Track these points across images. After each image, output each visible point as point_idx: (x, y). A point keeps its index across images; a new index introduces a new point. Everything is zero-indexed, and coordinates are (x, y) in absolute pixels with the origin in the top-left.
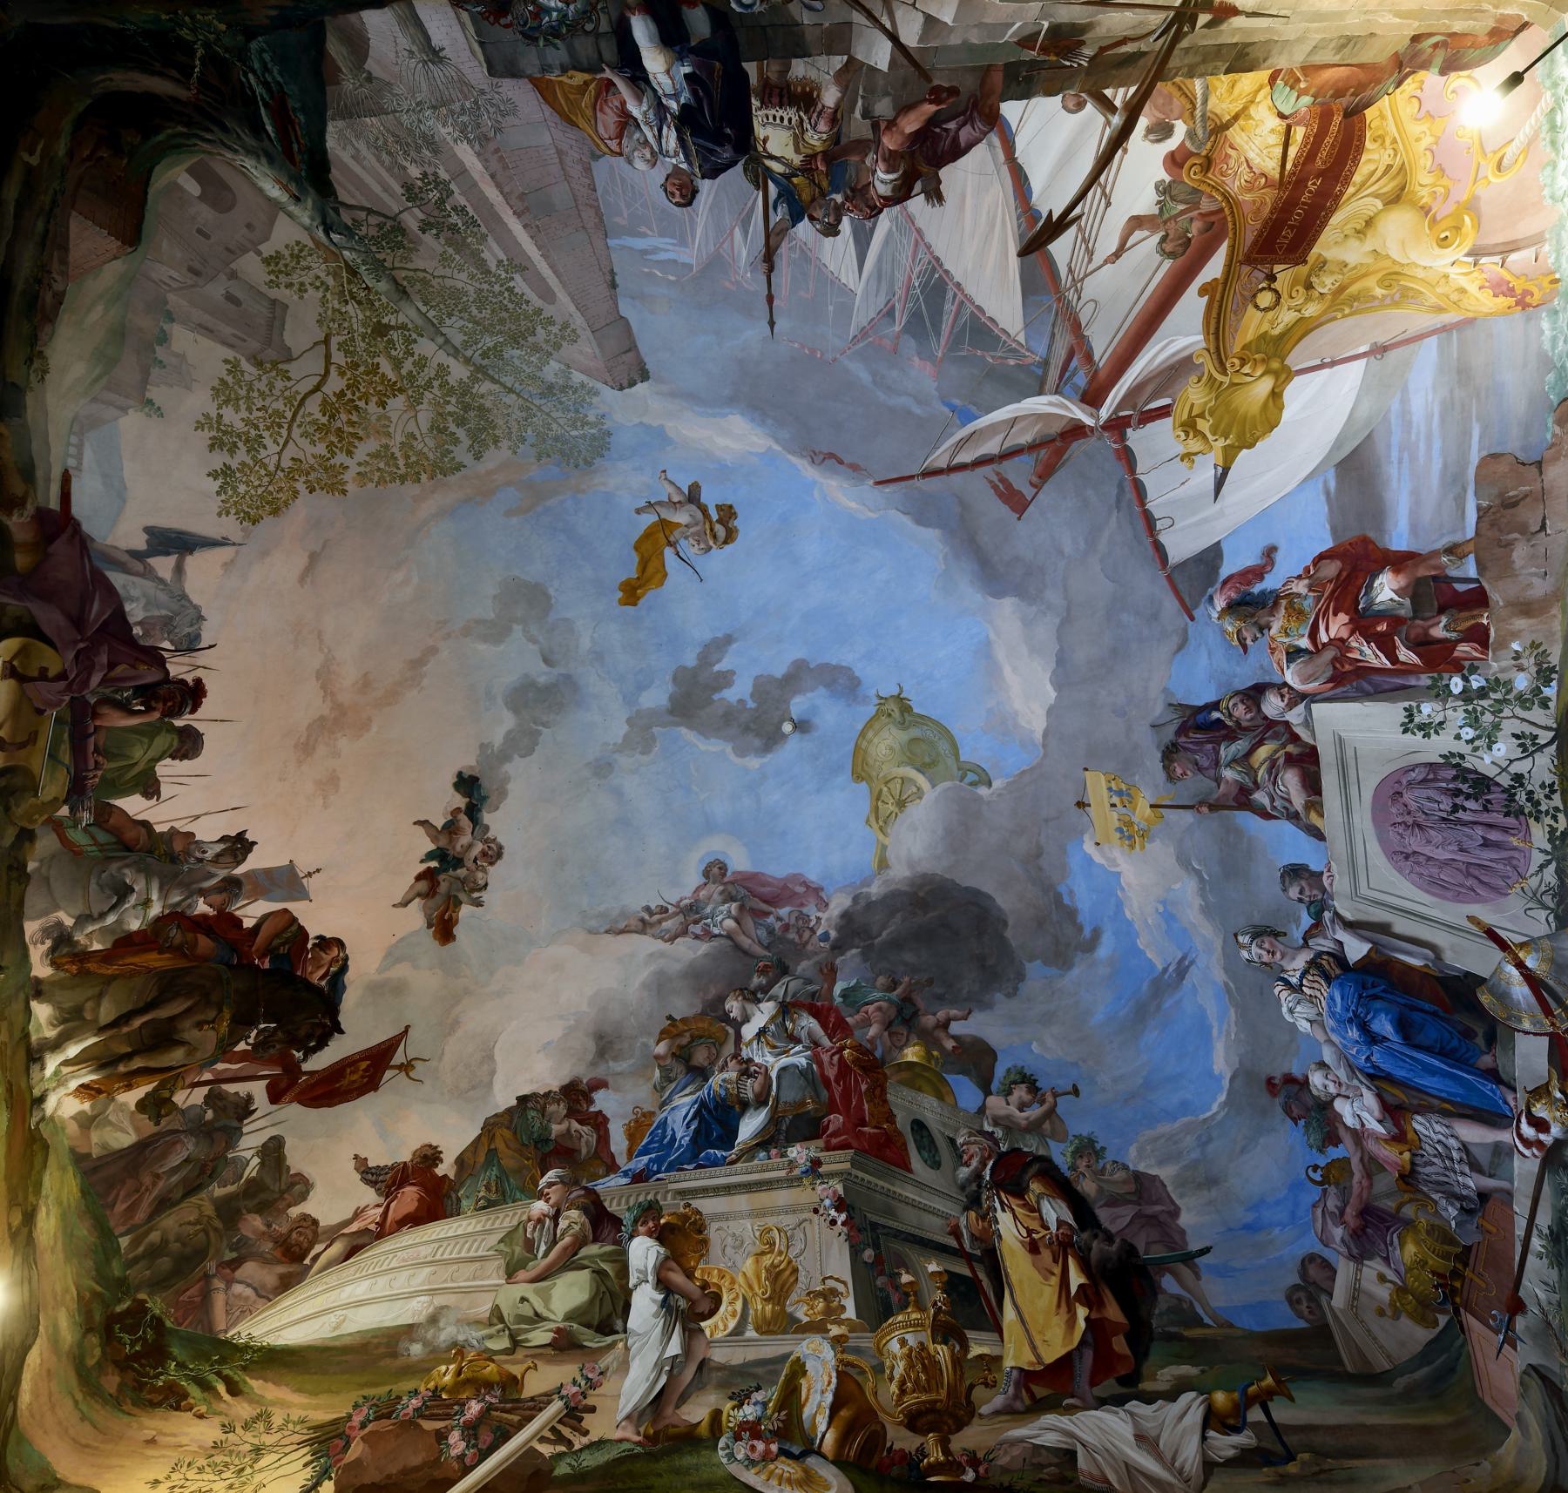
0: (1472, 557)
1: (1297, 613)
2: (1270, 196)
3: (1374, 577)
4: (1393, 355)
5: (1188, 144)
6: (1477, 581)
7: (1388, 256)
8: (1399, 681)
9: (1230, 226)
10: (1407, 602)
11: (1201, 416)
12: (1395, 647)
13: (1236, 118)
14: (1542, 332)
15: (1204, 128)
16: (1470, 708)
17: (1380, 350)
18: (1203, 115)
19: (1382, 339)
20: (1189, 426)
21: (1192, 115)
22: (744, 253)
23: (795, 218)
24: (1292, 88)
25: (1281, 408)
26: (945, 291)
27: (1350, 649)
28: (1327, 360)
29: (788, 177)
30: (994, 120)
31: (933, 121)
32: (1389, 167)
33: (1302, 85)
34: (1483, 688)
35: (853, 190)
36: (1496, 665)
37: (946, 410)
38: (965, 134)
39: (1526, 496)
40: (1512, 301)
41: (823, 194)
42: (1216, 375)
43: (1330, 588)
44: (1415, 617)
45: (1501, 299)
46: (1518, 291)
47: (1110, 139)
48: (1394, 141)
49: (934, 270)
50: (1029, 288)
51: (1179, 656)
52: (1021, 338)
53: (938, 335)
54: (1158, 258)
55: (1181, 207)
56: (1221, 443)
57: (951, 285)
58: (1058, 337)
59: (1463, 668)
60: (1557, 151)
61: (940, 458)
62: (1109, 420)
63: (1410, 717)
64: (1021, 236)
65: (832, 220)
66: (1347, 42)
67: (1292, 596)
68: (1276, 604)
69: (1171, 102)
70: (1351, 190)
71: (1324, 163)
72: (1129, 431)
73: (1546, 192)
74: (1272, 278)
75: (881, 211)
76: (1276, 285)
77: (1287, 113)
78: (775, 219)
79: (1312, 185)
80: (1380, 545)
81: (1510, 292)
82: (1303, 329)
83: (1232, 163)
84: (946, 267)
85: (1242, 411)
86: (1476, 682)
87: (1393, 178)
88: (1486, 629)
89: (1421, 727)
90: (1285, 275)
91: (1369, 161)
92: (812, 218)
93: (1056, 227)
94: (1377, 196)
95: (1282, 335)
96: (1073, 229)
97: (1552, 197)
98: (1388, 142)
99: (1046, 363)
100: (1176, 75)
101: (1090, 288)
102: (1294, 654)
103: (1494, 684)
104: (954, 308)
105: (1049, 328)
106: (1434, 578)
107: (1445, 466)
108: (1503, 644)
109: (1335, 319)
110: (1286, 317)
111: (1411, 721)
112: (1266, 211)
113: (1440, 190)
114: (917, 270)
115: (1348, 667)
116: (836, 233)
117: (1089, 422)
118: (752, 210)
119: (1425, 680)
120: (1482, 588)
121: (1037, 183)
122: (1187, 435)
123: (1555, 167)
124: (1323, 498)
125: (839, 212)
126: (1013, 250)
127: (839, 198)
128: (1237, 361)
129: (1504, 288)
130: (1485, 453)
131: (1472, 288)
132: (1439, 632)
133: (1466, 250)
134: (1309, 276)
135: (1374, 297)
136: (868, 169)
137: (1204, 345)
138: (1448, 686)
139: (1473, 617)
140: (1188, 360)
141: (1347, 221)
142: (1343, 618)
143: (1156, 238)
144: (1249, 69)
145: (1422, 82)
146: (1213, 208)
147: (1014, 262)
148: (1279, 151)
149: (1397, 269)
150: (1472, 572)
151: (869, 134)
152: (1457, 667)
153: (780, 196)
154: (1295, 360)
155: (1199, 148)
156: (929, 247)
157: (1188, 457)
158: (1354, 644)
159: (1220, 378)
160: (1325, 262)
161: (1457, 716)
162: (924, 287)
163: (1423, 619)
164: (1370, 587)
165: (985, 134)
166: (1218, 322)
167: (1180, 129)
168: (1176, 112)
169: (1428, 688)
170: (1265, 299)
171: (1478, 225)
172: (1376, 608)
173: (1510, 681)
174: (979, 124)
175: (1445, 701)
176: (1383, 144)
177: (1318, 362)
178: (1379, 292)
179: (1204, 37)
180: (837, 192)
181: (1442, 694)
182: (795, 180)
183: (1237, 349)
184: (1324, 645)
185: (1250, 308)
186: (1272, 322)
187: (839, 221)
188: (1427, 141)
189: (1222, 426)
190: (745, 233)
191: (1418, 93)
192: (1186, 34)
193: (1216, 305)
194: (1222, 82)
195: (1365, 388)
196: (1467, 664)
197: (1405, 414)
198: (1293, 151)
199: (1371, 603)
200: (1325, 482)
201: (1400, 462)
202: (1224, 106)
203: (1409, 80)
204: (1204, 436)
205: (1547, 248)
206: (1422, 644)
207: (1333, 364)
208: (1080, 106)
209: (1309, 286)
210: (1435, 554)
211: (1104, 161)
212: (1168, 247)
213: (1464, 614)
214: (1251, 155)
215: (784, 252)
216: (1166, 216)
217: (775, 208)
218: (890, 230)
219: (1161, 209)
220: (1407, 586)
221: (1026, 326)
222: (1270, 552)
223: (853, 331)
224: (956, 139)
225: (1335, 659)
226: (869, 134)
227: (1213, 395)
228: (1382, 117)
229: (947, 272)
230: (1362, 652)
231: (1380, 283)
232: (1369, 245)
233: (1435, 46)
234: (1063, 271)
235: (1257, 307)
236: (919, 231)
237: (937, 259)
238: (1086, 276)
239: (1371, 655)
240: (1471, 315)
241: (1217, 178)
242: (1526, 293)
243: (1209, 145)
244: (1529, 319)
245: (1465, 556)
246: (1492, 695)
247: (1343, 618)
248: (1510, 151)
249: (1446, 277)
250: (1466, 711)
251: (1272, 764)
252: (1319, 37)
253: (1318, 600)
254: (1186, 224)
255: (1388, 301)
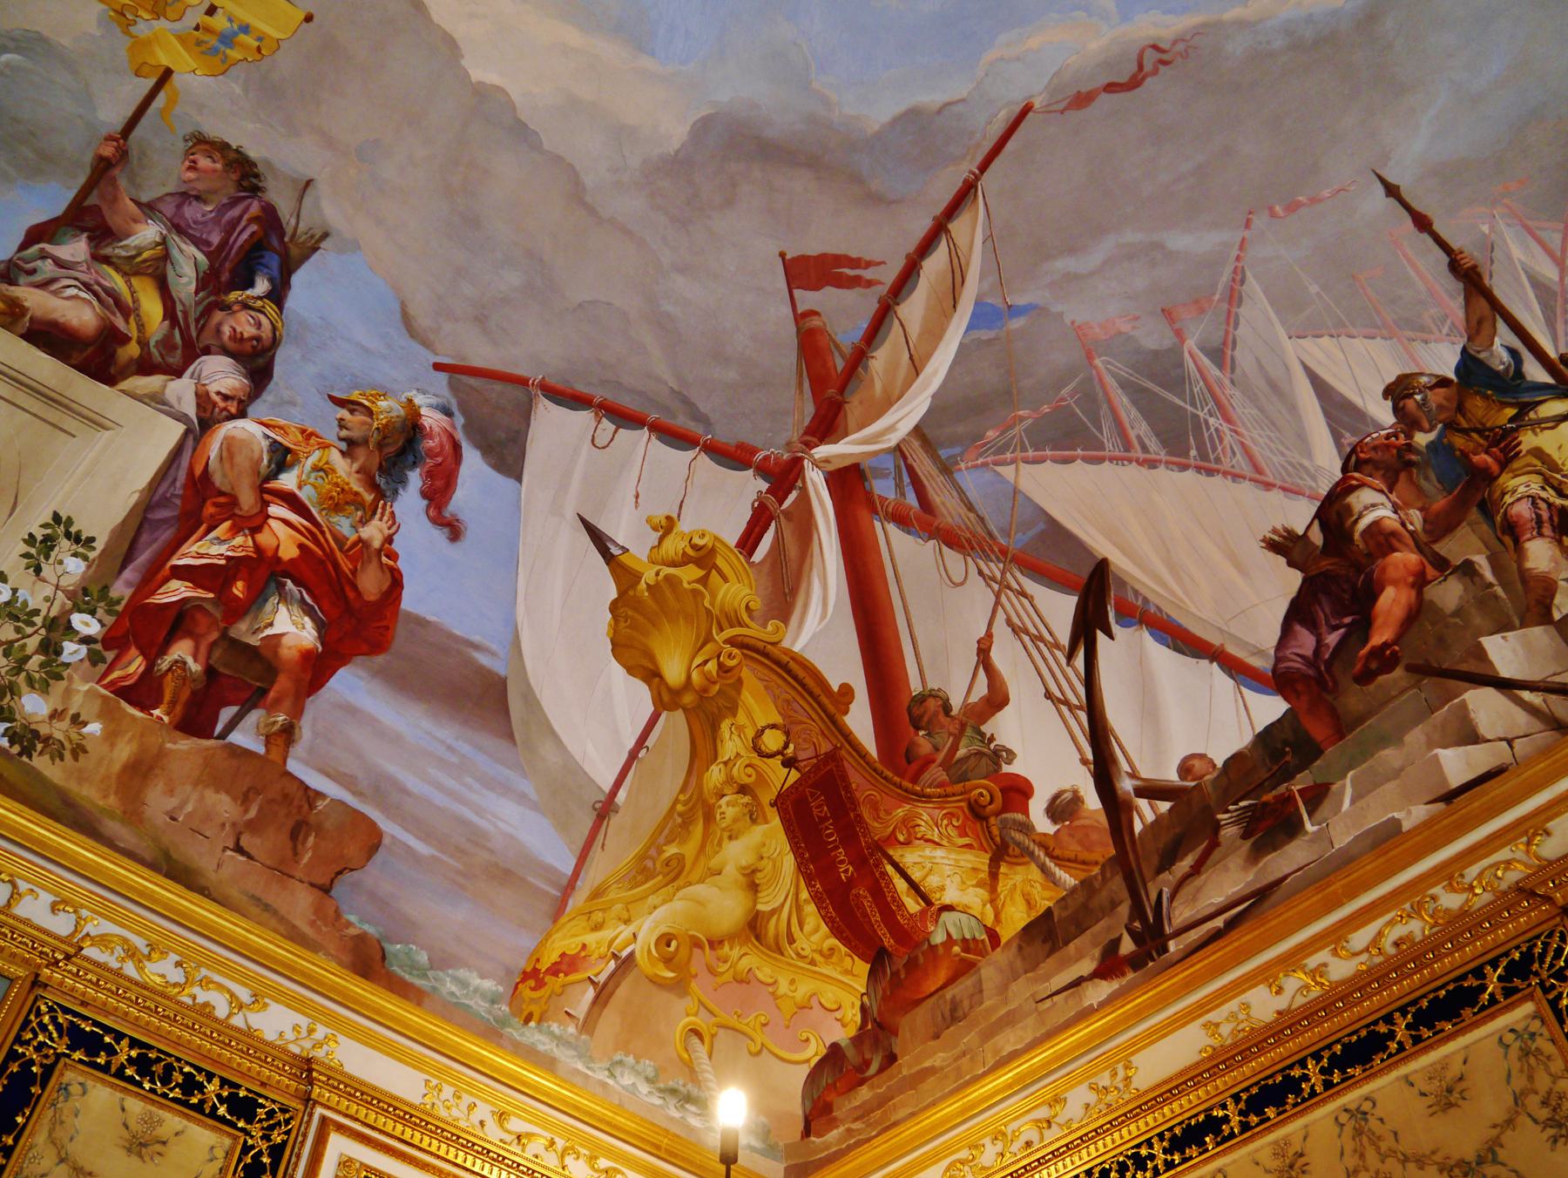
0: (261, 750)
1: (340, 501)
2: (878, 829)
3: (320, 626)
4: (587, 822)
5: (1019, 817)
6: (223, 736)
7: (701, 881)
8: (143, 558)
9: (889, 774)
10: (254, 641)
11: (704, 580)
12: (198, 585)
13: (994, 875)
14: (482, 977)
15: (1018, 844)
16: (38, 620)
17: (605, 809)
18: (1031, 854)
19: (615, 821)
20: (703, 557)
21: (1042, 845)
22: (1517, 253)
23: (1470, 366)
24: (964, 940)
25: (631, 670)
26: (1165, 443)
27: (236, 530)
28: (642, 753)
29: (1525, 408)
30: (1279, 681)
31: (1364, 624)
32: (791, 940)
33: (956, 949)
34: (59, 652)
35: (1410, 464)
36: (83, 690)
37: (1020, 300)
38: (1305, 641)
39: (295, 853)
40: (543, 966)
41: (1450, 426)
42: (737, 631)
43: (346, 566)
44: (224, 635)
45: (555, 957)
46: (548, 979)
47: (1115, 761)
48: (813, 963)
49: (1203, 455)
50: (1055, 533)
51: (398, 316)
52: (1007, 472)
53: (1124, 385)
54: (933, 684)
55: (961, 752)
56: (649, 576)
57: (1163, 455)
58: (963, 511)
59: (107, 647)
60: (660, 1090)
61: (969, 230)
62: (800, 472)
63: (77, 539)
64: (1122, 583)
65: (1410, 404)
66: (954, 1015)
67: (370, 513)
68: (373, 486)
69: (1080, 842)
70: (805, 895)
71: (858, 896)
72: (764, 486)
73: (630, 1060)
74: (789, 763)
75: (1345, 469)
76: (777, 761)
77: (945, 916)
78: (1504, 336)
79: (846, 870)
80: (359, 659)
81: (554, 970)
82: (703, 749)
83: (953, 832)
84: (1190, 474)
85: (667, 627)
86: (72, 651)
87: (777, 937)
88: (144, 708)
89: (48, 543)
90: (779, 777)
91: (816, 930)
92: (1443, 382)
93: (1088, 626)
94: (773, 912)
95: (715, 728)
96: (1064, 638)
97: (620, 1062)
98: (818, 957)
99: (946, 469)
100: (1103, 872)
101: (978, 597)
102: (282, 458)
103: (54, 672)
104: (1132, 434)
105: (983, 512)
106: (264, 692)
107: (404, 791)
108: (107, 713)
109: (683, 790)
110: (732, 745)
111: (68, 535)
112: (866, 813)
113: (723, 968)
114: (1228, 438)
115: (209, 509)
116: (1388, 392)
117: (822, 451)
118: (1550, 323)
119: (121, 590)
120: (209, 736)
121: (1161, 656)
122: (695, 547)
123: (648, 1080)
124: (476, 638)
125: (1408, 422)
126: (1118, 560)
127: (1422, 439)
128: (731, 663)
129: (564, 967)
130: (386, 841)
131: (591, 939)
132: (181, 650)
133: (638, 955)
134: (755, 797)
135: (669, 842)
136: (1408, 505)
137: (785, 644)
138: (92, 613)
139: (173, 703)
140: (785, 617)
141: (777, 870)
142: (289, 552)
143: (956, 702)
144: (1027, 929)
145: (844, 1026)
146: (927, 776)
147: (1102, 547)
148: (916, 875)
149: (680, 882)
150: (236, 737)
151: (1446, 548)
152: (114, 640)
153: (1519, 373)
154: (675, 725)
155: (1004, 821)
156: (1236, 477)
157: (667, 527)
158: (239, 540)
159: (729, 632)
160: (754, 821)
161: (35, 596)
162: (1198, 425)
163: (213, 645)
164: (308, 611)
165: (1278, 660)
166: (795, 678)
167: (1043, 824)
168: (1065, 838)
169: (105, 589)
170: (773, 741)
171: (656, 982)
172: (274, 600)
173: (44, 689)
174: (1297, 665)
175: (70, 595)
176: (821, 953)
177: (650, 742)
178: (671, 850)
179: (1109, 929)
180: (1430, 446)
181: (84, 597)
182: (1510, 412)
183: (746, 673)
184: (266, 504)
185: (778, 720)
186: (741, 729)
187: (1396, 410)
188: (783, 987)
189: (668, 592)
190: (1538, 285)
191: (838, 1015)
192: (1131, 919)
193: (817, 691)
194: (1044, 899)
195: (573, 769)
196: (110, 656)
197: (505, 790)
198: (901, 885)
199: (284, 598)
200: (493, 654)
201: (450, 748)
202: (1019, 878)
203: (858, 1019)
204: (674, 564)
205: (572, 1029)
206: (180, 620)
207: (633, 756)
208: (1185, 769)
209: (743, 790)
210: (297, 712)
211: (1099, 733)
212: (932, 704)
213: (185, 695)
214: (939, 853)
215: (1451, 300)
216: (969, 732)
217: (1513, 353)
218: (1310, 455)
219: (982, 735)
220: (276, 653)
221: (1016, 491)
222: (454, 530)
223: (1253, 286)
224: (1313, 626)
225: (234, 501)
226: (1446, 548)
227: (716, 611)
228: (847, 972)
229: (1184, 467)
230: (221, 541)
231: (680, 858)
232: (731, 871)
233: (867, 1064)
234: (1030, 586)
235: (773, 726)
236: (1268, 486)
237: (1210, 472)
238: (998, 603)
239: (211, 548)
240: (563, 920)
241: (950, 808)
242: (540, 984)
243: (995, 831)
244: (509, 972)
245: (268, 743)
246: (37, 659)
247: (289, 552)
248: (701, 1051)
249: (627, 922)
250: (36, 612)
251: (126, 311)
252: (987, 1003)
253: (340, 540)
254: (938, 739)
255: (653, 852)
